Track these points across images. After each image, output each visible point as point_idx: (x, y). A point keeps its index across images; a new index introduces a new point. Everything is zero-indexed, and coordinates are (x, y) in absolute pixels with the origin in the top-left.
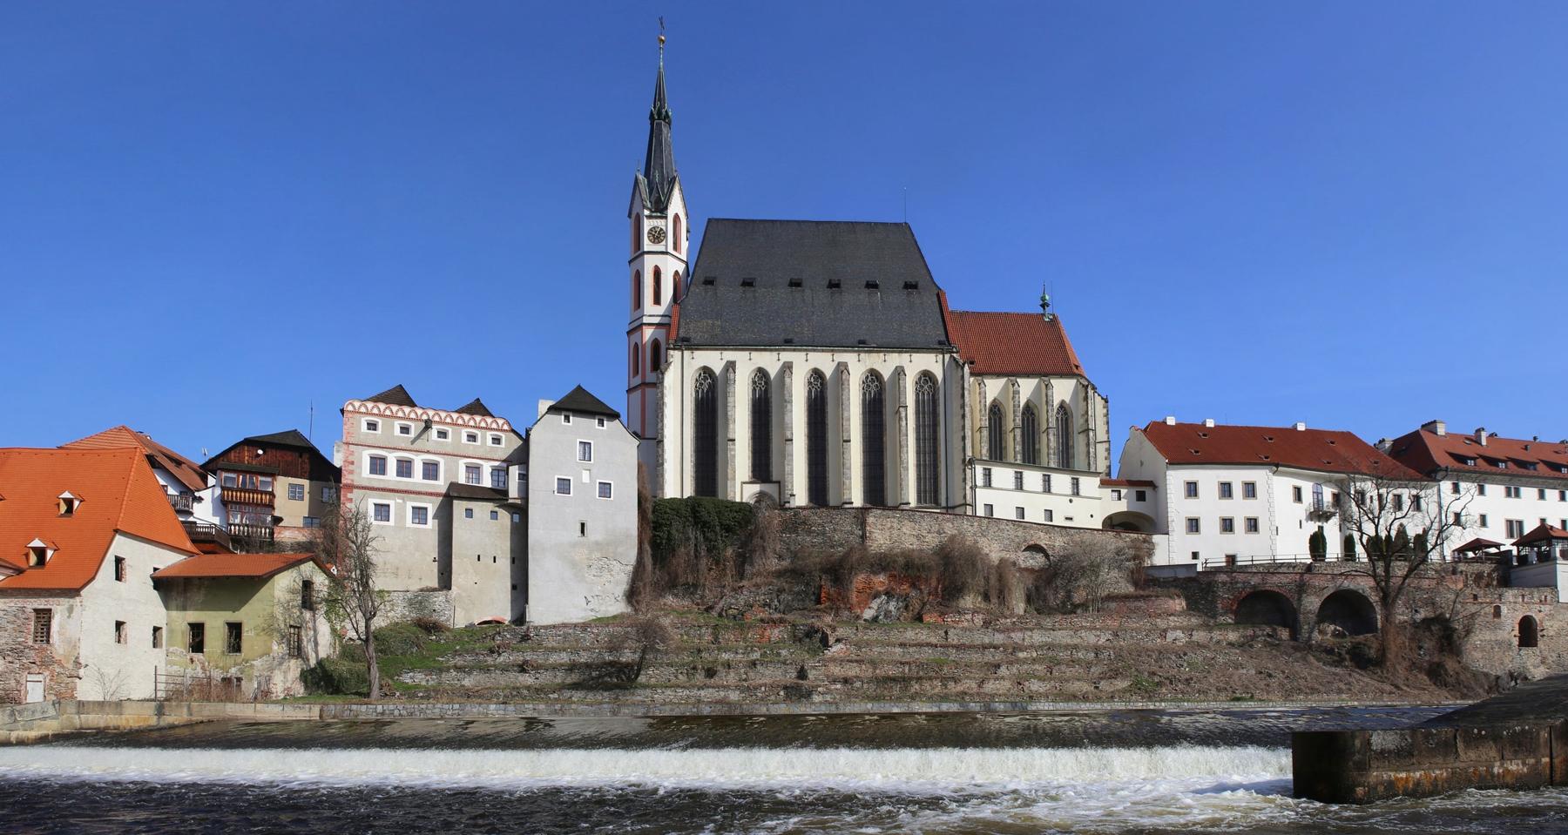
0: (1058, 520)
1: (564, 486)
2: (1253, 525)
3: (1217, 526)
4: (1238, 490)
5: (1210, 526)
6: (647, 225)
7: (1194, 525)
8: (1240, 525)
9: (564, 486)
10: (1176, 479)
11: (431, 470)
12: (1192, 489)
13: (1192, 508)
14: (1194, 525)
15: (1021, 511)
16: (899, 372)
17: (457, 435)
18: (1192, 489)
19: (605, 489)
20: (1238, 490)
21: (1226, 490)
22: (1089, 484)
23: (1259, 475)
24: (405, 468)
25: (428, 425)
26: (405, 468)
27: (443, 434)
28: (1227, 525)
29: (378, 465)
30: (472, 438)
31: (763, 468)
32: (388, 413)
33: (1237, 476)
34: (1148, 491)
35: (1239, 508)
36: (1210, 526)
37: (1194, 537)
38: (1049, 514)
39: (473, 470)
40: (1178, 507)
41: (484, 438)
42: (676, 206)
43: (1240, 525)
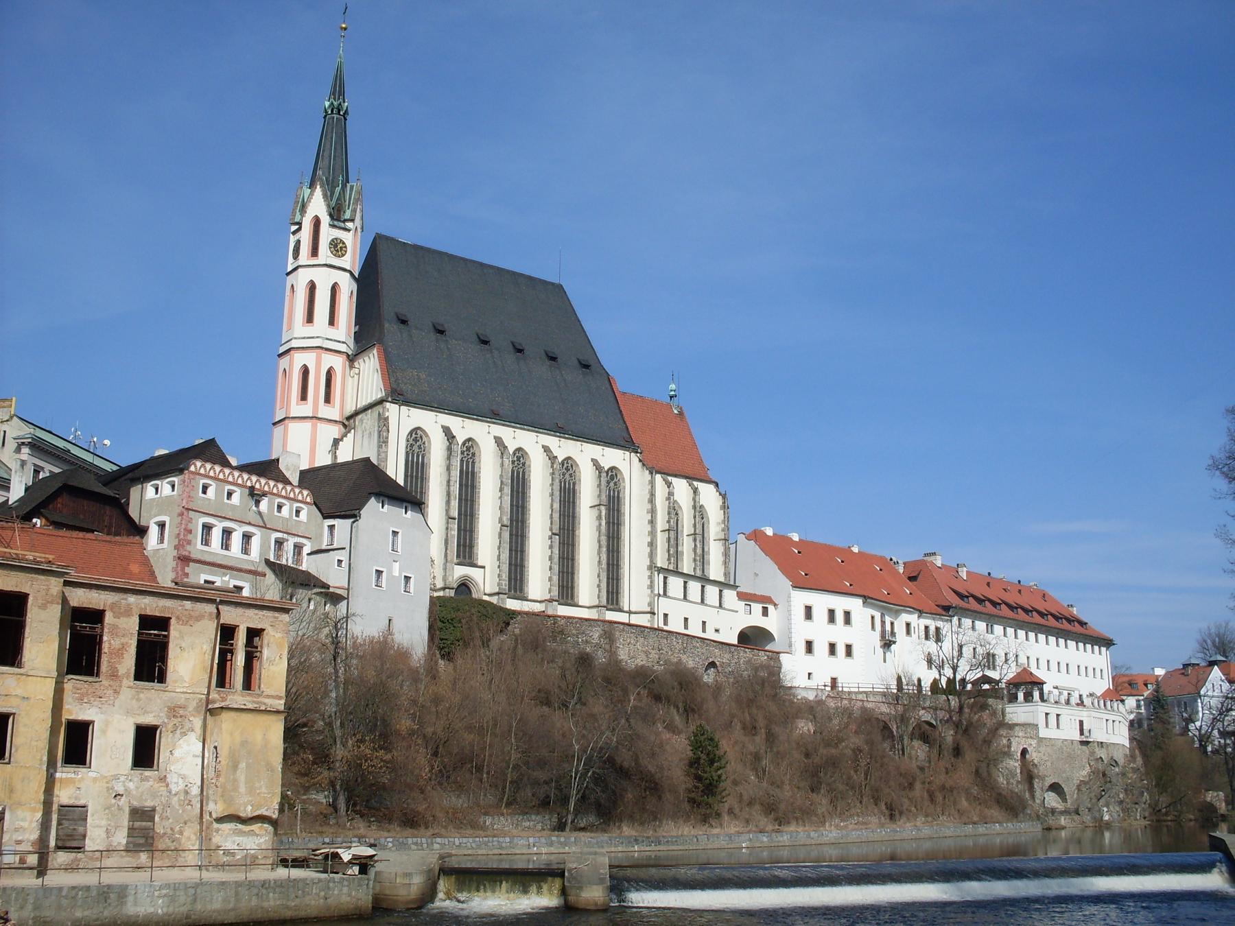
0: (710, 635)
2: (849, 649)
4: (840, 617)
5: (821, 648)
6: (327, 233)
7: (809, 646)
14: (809, 646)
20: (840, 617)
22: (730, 595)
23: (854, 605)
28: (832, 648)
32: (221, 476)
33: (841, 603)
34: (771, 608)
35: (840, 634)
36: (821, 648)
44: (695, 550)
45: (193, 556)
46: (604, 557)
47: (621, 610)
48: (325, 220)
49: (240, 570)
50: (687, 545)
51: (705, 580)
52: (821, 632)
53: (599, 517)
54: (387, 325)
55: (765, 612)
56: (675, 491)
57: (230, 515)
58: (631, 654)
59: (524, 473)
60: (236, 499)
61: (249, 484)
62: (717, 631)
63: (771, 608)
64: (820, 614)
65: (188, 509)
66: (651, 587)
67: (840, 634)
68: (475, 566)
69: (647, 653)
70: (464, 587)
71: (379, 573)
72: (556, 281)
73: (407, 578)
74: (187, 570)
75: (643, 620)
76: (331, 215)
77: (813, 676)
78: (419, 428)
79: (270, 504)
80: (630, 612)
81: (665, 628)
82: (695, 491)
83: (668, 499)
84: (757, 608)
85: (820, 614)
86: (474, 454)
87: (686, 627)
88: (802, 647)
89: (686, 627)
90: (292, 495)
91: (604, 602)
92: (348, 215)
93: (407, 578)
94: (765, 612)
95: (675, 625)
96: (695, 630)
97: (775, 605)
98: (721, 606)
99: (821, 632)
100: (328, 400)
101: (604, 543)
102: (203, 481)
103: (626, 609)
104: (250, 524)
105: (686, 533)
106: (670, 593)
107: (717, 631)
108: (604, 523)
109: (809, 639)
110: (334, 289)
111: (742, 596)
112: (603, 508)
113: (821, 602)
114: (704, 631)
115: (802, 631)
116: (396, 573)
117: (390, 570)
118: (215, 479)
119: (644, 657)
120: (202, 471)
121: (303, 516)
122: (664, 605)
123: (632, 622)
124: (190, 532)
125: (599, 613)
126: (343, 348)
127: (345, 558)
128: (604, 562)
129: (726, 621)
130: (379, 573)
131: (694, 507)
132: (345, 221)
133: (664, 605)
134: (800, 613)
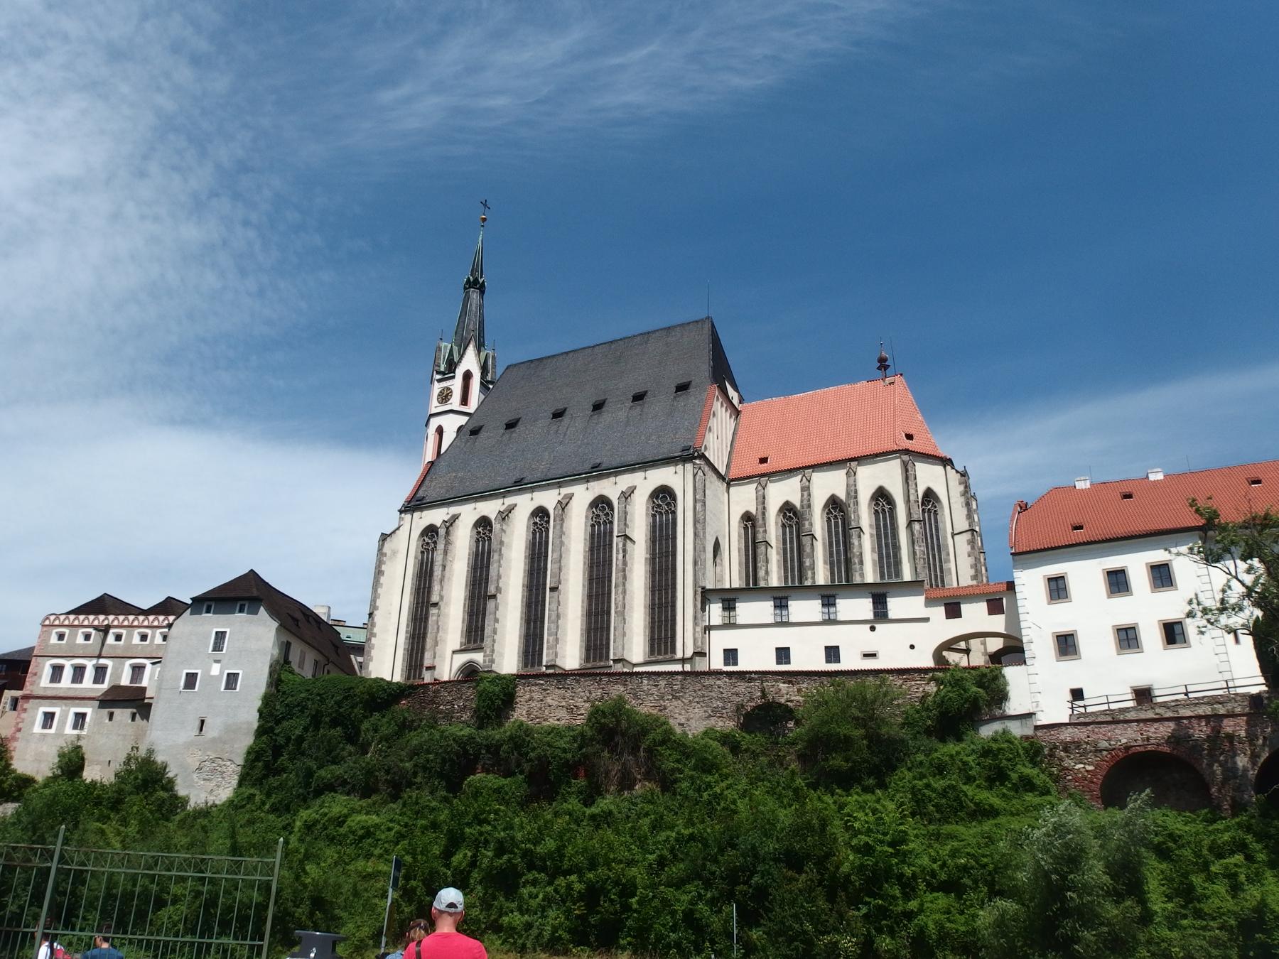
1: (191, 680)
7: (1066, 644)
8: (1151, 636)
9: (191, 680)
11: (100, 672)
12: (1057, 588)
13: (1062, 617)
14: (1066, 644)
15: (783, 654)
16: (626, 495)
17: (130, 636)
18: (1057, 588)
19: (232, 679)
21: (1118, 582)
24: (79, 672)
25: (105, 630)
26: (79, 672)
27: (118, 638)
28: (1127, 638)
29: (57, 671)
30: (144, 638)
31: (475, 633)
37: (1068, 665)
38: (832, 653)
39: (138, 670)
40: (1039, 619)
41: (153, 637)
42: (470, 362)
57: (81, 653)
69: (570, 710)
107: (873, 655)
119: (563, 713)
129: (907, 640)
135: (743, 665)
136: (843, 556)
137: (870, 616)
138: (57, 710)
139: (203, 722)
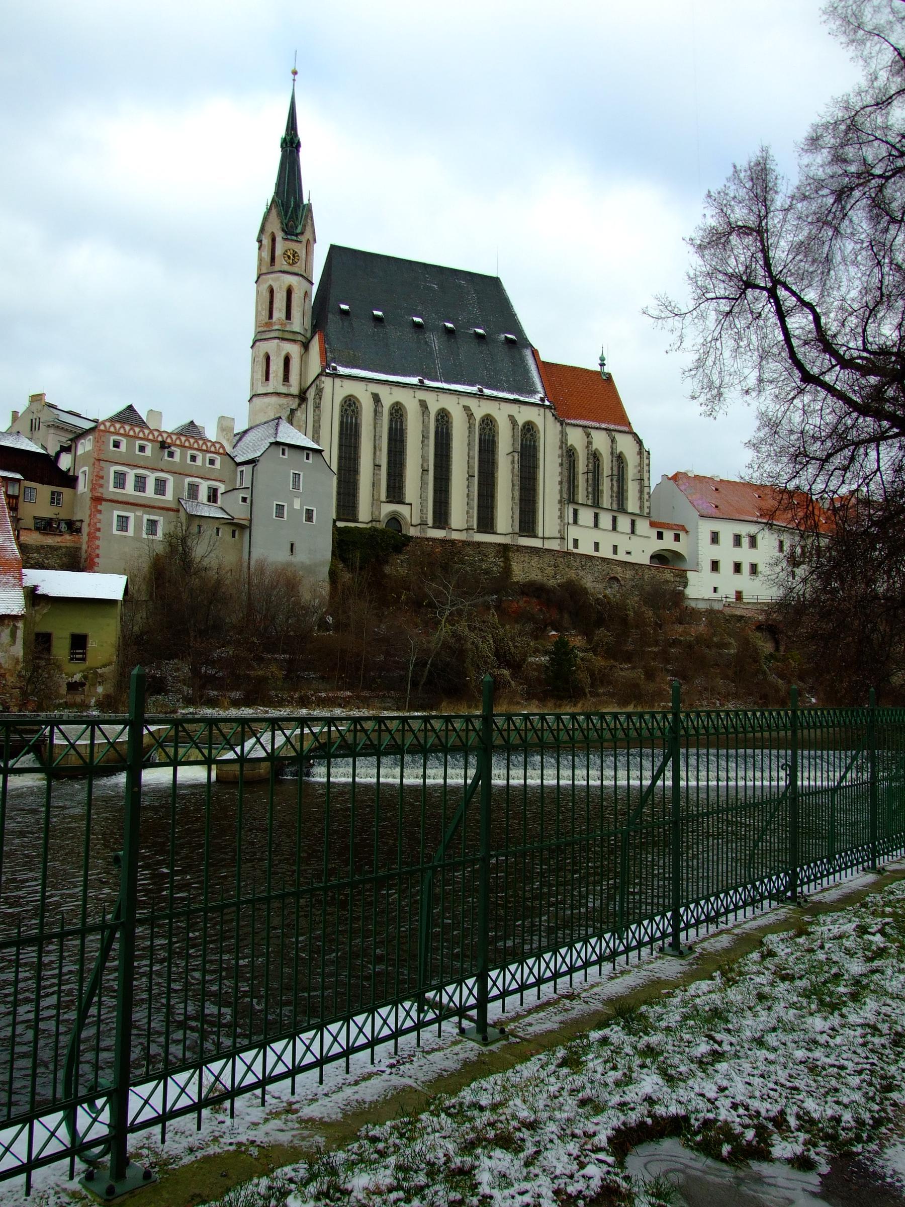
0: (621, 556)
3: (722, 566)
5: (726, 567)
7: (715, 566)
8: (746, 569)
10: (705, 528)
11: (160, 486)
12: (715, 538)
14: (715, 566)
18: (715, 538)
22: (643, 526)
24: (140, 483)
26: (140, 483)
28: (737, 568)
29: (120, 480)
32: (132, 433)
33: (745, 530)
35: (745, 555)
36: (726, 567)
43: (746, 569)
44: (612, 488)
45: (105, 496)
46: (517, 494)
47: (536, 536)
48: (279, 236)
49: (153, 507)
50: (606, 486)
51: (625, 512)
52: (726, 553)
53: (513, 462)
54: (330, 316)
55: (677, 538)
56: (594, 441)
57: (142, 463)
58: (522, 571)
59: (447, 429)
60: (148, 452)
61: (160, 439)
62: (629, 553)
63: (683, 535)
64: (726, 539)
65: (99, 460)
66: (561, 517)
67: (745, 555)
68: (403, 503)
69: (542, 570)
70: (395, 520)
71: (280, 508)
72: (494, 275)
73: (309, 513)
74: (99, 507)
75: (554, 545)
76: (283, 230)
77: (719, 590)
78: (351, 396)
79: (183, 456)
80: (543, 538)
81: (575, 551)
82: (613, 441)
83: (587, 447)
84: (669, 535)
85: (726, 539)
86: (402, 415)
87: (597, 549)
88: (708, 566)
89: (597, 549)
90: (204, 448)
91: (517, 530)
92: (299, 230)
93: (309, 513)
94: (677, 538)
95: (586, 549)
96: (606, 552)
97: (687, 532)
98: (633, 532)
99: (726, 553)
100: (286, 378)
101: (517, 483)
102: (113, 438)
103: (540, 535)
104: (162, 470)
105: (605, 474)
106: (580, 522)
107: (629, 553)
108: (516, 466)
109: (715, 558)
110: (289, 292)
111: (653, 525)
112: (516, 454)
113: (727, 530)
114: (615, 552)
115: (707, 552)
116: (297, 506)
117: (291, 505)
118: (126, 435)
119: (539, 572)
120: (112, 429)
121: (218, 465)
122: (573, 532)
123: (546, 547)
124: (102, 478)
125: (513, 538)
126: (299, 338)
127: (248, 496)
128: (517, 497)
129: (640, 547)
130: (280, 508)
131: (612, 453)
132: (297, 235)
133: (573, 532)
134: (705, 537)
135: (581, 550)
136: (620, 496)
137: (629, 531)
138: (131, 515)
139: (292, 545)
